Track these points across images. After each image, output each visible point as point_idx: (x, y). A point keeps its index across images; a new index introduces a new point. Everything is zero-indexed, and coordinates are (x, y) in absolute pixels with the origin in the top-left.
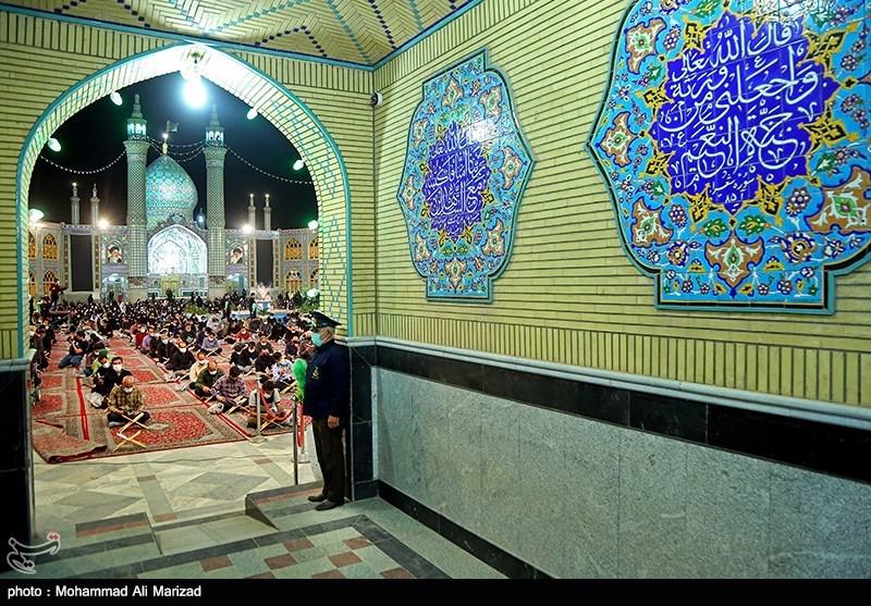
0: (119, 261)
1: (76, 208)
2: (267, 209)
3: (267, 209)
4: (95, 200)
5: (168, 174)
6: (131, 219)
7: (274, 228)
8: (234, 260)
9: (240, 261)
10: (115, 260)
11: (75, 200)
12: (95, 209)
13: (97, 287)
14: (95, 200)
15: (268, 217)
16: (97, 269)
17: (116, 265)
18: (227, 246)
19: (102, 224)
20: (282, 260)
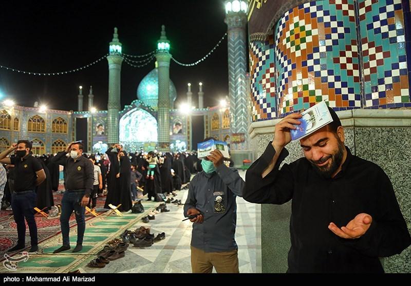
0: (103, 133)
1: (80, 102)
2: (201, 93)
3: (201, 93)
4: (91, 96)
5: (152, 79)
6: (109, 107)
7: (205, 106)
8: (176, 131)
9: (180, 132)
10: (100, 133)
11: (80, 96)
12: (90, 101)
13: (89, 150)
14: (91, 96)
15: (201, 99)
16: (90, 138)
17: (100, 136)
18: (170, 122)
19: (93, 110)
20: (210, 129)
